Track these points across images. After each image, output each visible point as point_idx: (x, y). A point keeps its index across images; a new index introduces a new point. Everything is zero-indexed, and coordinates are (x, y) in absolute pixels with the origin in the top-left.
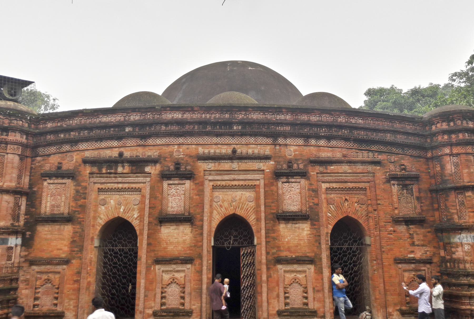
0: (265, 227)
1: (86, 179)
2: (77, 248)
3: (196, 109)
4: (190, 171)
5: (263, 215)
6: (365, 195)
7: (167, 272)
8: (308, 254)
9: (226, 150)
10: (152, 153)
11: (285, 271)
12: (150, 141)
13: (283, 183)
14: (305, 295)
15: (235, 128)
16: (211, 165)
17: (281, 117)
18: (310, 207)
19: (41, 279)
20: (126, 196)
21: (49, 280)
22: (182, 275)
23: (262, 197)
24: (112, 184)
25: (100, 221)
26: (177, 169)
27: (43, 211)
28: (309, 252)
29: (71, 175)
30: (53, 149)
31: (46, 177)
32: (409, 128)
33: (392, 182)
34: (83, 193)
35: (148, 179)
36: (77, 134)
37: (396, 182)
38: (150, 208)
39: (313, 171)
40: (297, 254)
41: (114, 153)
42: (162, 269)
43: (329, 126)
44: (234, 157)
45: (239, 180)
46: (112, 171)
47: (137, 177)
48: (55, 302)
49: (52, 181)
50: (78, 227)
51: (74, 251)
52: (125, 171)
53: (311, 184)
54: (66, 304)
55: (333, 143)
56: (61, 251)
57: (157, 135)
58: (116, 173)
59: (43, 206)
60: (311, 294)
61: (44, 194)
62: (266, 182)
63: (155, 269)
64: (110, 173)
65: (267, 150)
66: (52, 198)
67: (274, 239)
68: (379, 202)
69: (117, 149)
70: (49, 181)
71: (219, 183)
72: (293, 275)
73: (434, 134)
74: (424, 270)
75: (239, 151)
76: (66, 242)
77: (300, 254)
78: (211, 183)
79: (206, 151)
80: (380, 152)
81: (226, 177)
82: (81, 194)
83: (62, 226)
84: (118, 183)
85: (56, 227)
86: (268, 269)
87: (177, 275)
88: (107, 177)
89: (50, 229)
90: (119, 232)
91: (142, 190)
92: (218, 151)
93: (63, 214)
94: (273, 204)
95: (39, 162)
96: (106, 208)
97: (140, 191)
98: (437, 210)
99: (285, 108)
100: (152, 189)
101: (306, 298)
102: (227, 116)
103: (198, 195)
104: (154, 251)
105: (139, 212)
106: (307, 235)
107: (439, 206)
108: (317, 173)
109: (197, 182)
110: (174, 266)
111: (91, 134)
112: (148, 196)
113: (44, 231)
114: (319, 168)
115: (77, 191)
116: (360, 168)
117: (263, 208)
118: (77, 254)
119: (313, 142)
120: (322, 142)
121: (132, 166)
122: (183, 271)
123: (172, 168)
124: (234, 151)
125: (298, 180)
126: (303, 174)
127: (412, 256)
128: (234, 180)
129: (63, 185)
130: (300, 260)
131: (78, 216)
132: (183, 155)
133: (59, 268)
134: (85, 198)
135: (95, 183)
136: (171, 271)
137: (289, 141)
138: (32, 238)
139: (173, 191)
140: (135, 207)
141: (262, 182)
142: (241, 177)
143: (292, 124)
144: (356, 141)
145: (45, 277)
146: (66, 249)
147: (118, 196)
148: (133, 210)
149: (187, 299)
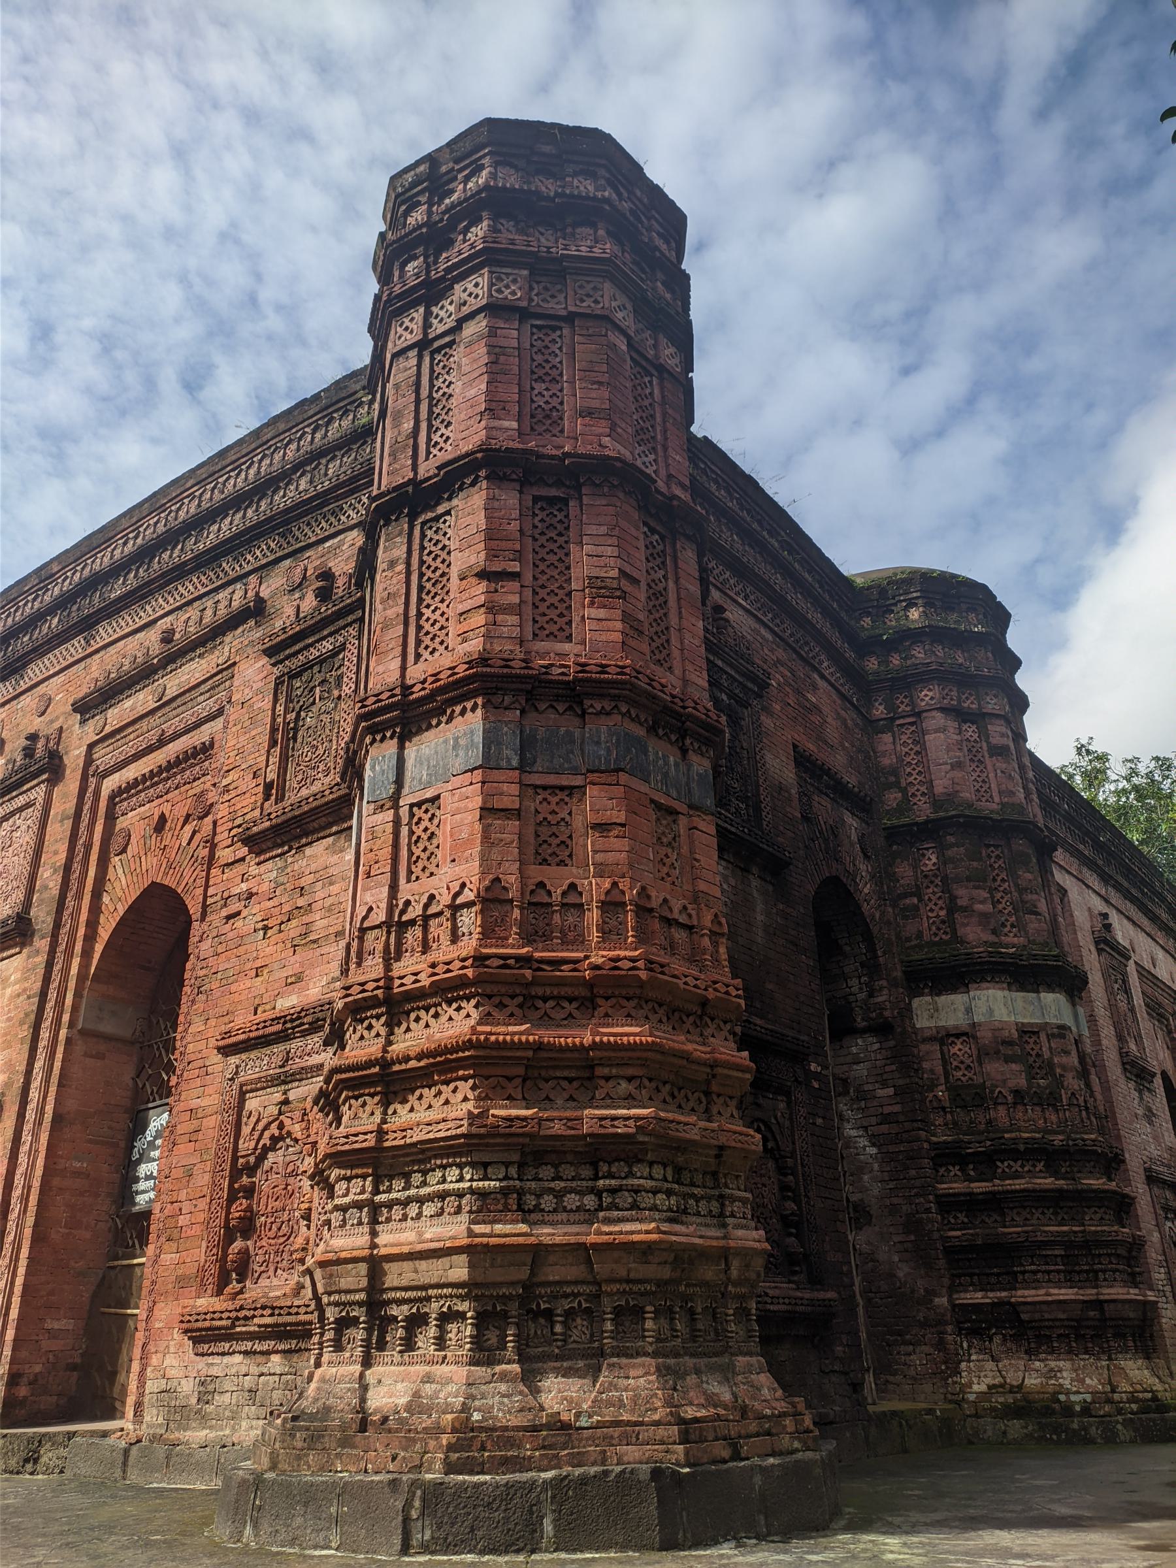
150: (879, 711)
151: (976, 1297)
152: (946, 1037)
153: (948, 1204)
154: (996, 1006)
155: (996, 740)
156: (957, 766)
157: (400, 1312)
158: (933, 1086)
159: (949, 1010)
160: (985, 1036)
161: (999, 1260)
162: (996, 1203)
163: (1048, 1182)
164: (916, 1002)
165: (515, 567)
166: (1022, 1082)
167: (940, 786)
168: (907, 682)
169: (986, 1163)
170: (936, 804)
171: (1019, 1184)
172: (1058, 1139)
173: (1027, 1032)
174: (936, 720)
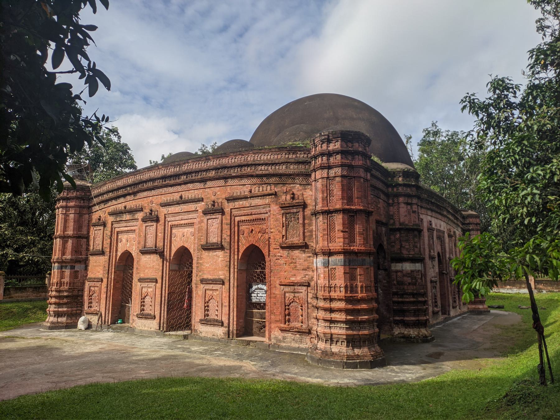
3: (160, 167)
9: (176, 197)
13: (208, 219)
22: (152, 289)
26: (151, 214)
28: (222, 274)
30: (97, 208)
41: (121, 207)
43: (241, 166)
44: (182, 201)
67: (201, 264)
71: (174, 223)
72: (211, 292)
74: (302, 292)
75: (183, 197)
76: (101, 267)
77: (217, 277)
80: (276, 184)
81: (177, 218)
86: (196, 287)
100: (139, 229)
103: (161, 233)
106: (221, 261)
108: (231, 209)
109: (160, 223)
114: (232, 205)
120: (236, 182)
124: (181, 197)
125: (217, 216)
127: (293, 279)
142: (186, 217)
143: (216, 169)
144: (258, 176)
150: (391, 201)
151: (398, 318)
152: (397, 272)
153: (394, 302)
154: (408, 267)
155: (414, 209)
156: (406, 216)
157: (335, 340)
158: (394, 281)
159: (398, 266)
160: (404, 272)
161: (403, 312)
162: (403, 302)
163: (412, 299)
164: (392, 264)
165: (347, 230)
166: (410, 281)
167: (402, 220)
168: (397, 195)
169: (402, 296)
170: (400, 224)
171: (407, 300)
172: (415, 292)
173: (412, 271)
174: (402, 205)
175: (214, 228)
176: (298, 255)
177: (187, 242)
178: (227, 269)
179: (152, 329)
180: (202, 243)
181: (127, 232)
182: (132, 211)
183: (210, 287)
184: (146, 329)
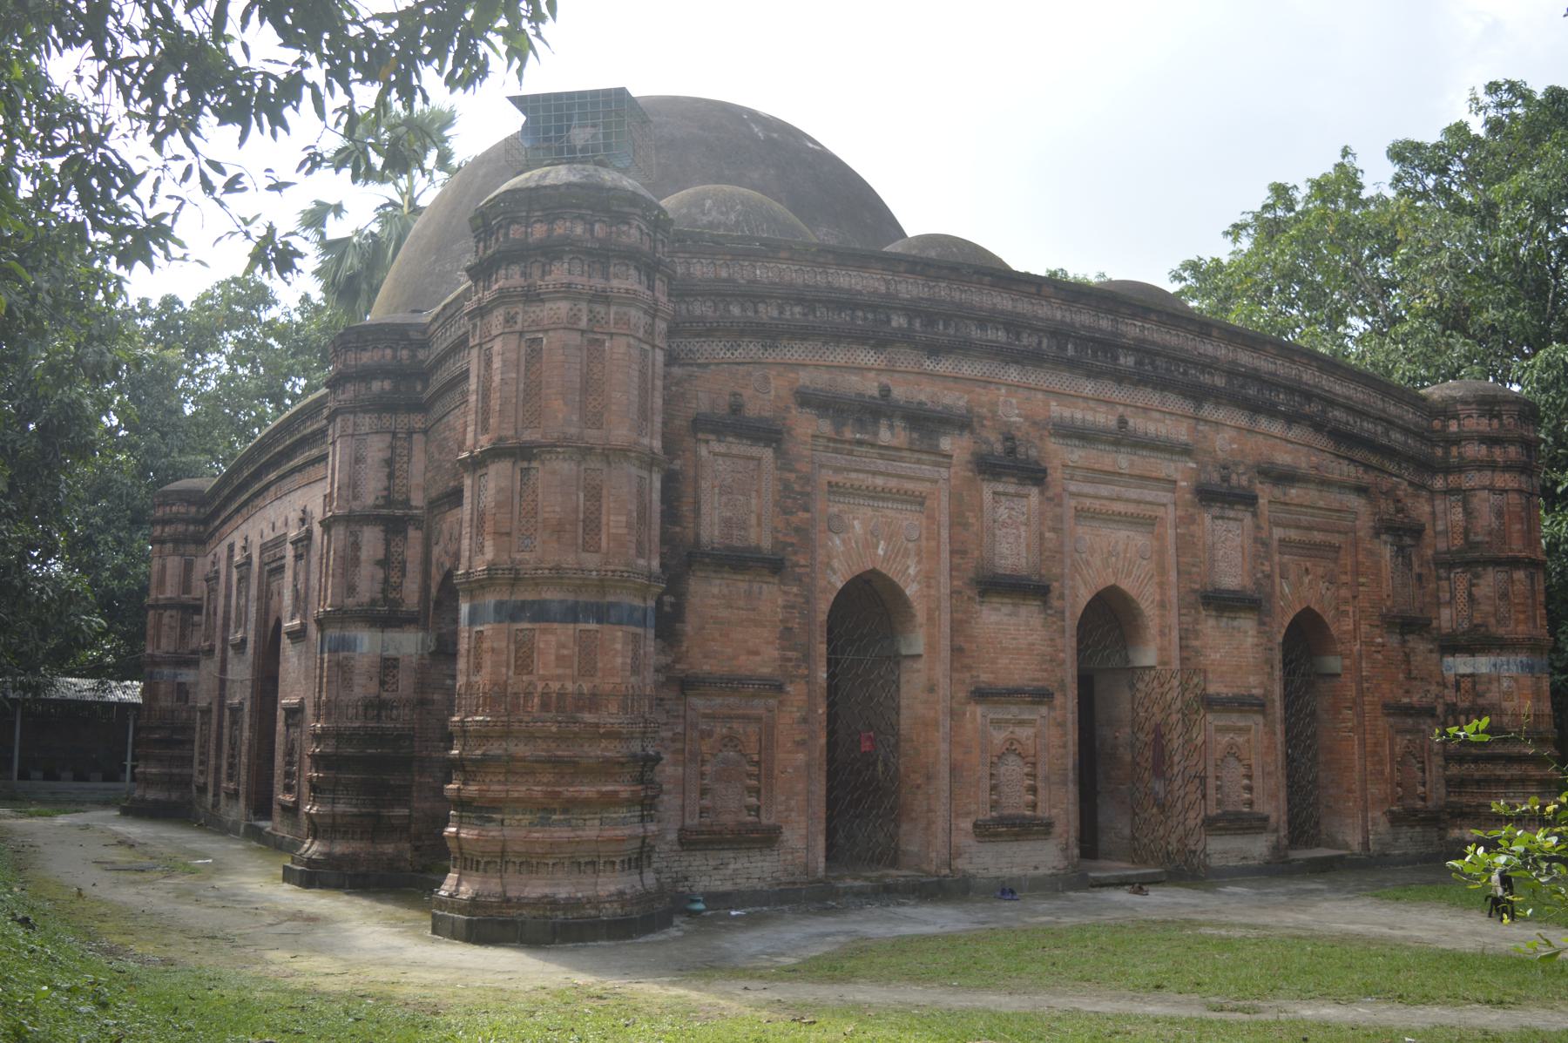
0: (1180, 623)
1: (806, 453)
2: (795, 650)
4: (1036, 462)
5: (1173, 593)
6: (1336, 560)
7: (997, 723)
8: (1254, 691)
9: (1104, 418)
10: (954, 399)
11: (1219, 730)
12: (945, 366)
13: (1215, 518)
14: (1246, 782)
15: (1122, 360)
16: (1077, 455)
17: (1208, 348)
18: (1257, 583)
19: (710, 734)
20: (888, 512)
21: (731, 739)
23: (1171, 550)
24: (861, 476)
25: (833, 579)
27: (705, 537)
28: (1253, 684)
29: (769, 433)
31: (712, 432)
32: (1410, 416)
33: (1384, 537)
34: (801, 493)
35: (944, 472)
36: (775, 314)
37: (1390, 539)
38: (952, 552)
39: (1265, 493)
40: (1236, 690)
42: (991, 716)
44: (1123, 438)
45: (1128, 500)
46: (866, 437)
47: (919, 461)
48: (753, 800)
49: (721, 448)
50: (795, 590)
51: (790, 660)
52: (895, 442)
53: (1258, 527)
54: (781, 808)
55: (1295, 433)
56: (758, 658)
57: (963, 348)
58: (873, 445)
59: (705, 520)
60: (1258, 783)
61: (704, 485)
62: (1180, 513)
63: (973, 714)
64: (860, 443)
65: (1180, 432)
66: (724, 499)
68: (1362, 580)
69: (872, 374)
70: (718, 447)
71: (1088, 502)
73: (1457, 441)
75: (1131, 422)
77: (1243, 691)
78: (1073, 503)
79: (1067, 413)
81: (1104, 490)
82: (794, 497)
83: (756, 586)
84: (874, 473)
85: (741, 584)
87: (1024, 733)
88: (850, 453)
89: (725, 591)
90: (868, 610)
91: (928, 502)
92: (1089, 417)
93: (758, 548)
94: (1195, 570)
95: (677, 384)
96: (843, 541)
97: (922, 504)
98: (1449, 603)
99: (1219, 328)
101: (1249, 789)
102: (1105, 324)
104: (969, 668)
105: (919, 562)
107: (1453, 597)
109: (1050, 494)
110: (1014, 709)
111: (811, 318)
112: (945, 519)
113: (709, 594)
115: (787, 486)
116: (1334, 498)
117: (1173, 576)
118: (799, 667)
119: (1264, 423)
120: (1277, 428)
121: (912, 429)
122: (1031, 723)
123: (999, 448)
124: (1123, 422)
125: (1240, 515)
126: (1248, 500)
128: (1118, 499)
129: (752, 465)
130: (1242, 704)
131: (794, 558)
132: (1019, 415)
133: (758, 707)
134: (807, 510)
135: (822, 466)
136: (1007, 721)
137: (1220, 414)
138: (678, 612)
139: (1003, 513)
140: (910, 545)
141: (1171, 514)
143: (1232, 372)
145: (721, 730)
146: (771, 652)
147: (870, 512)
148: (906, 554)
149: (1042, 794)
175: (1229, 549)
176: (1411, 645)
177: (1129, 574)
178: (1267, 669)
179: (1042, 871)
180: (1197, 586)
181: (875, 495)
182: (927, 423)
183: (1235, 720)
184: (1016, 871)
